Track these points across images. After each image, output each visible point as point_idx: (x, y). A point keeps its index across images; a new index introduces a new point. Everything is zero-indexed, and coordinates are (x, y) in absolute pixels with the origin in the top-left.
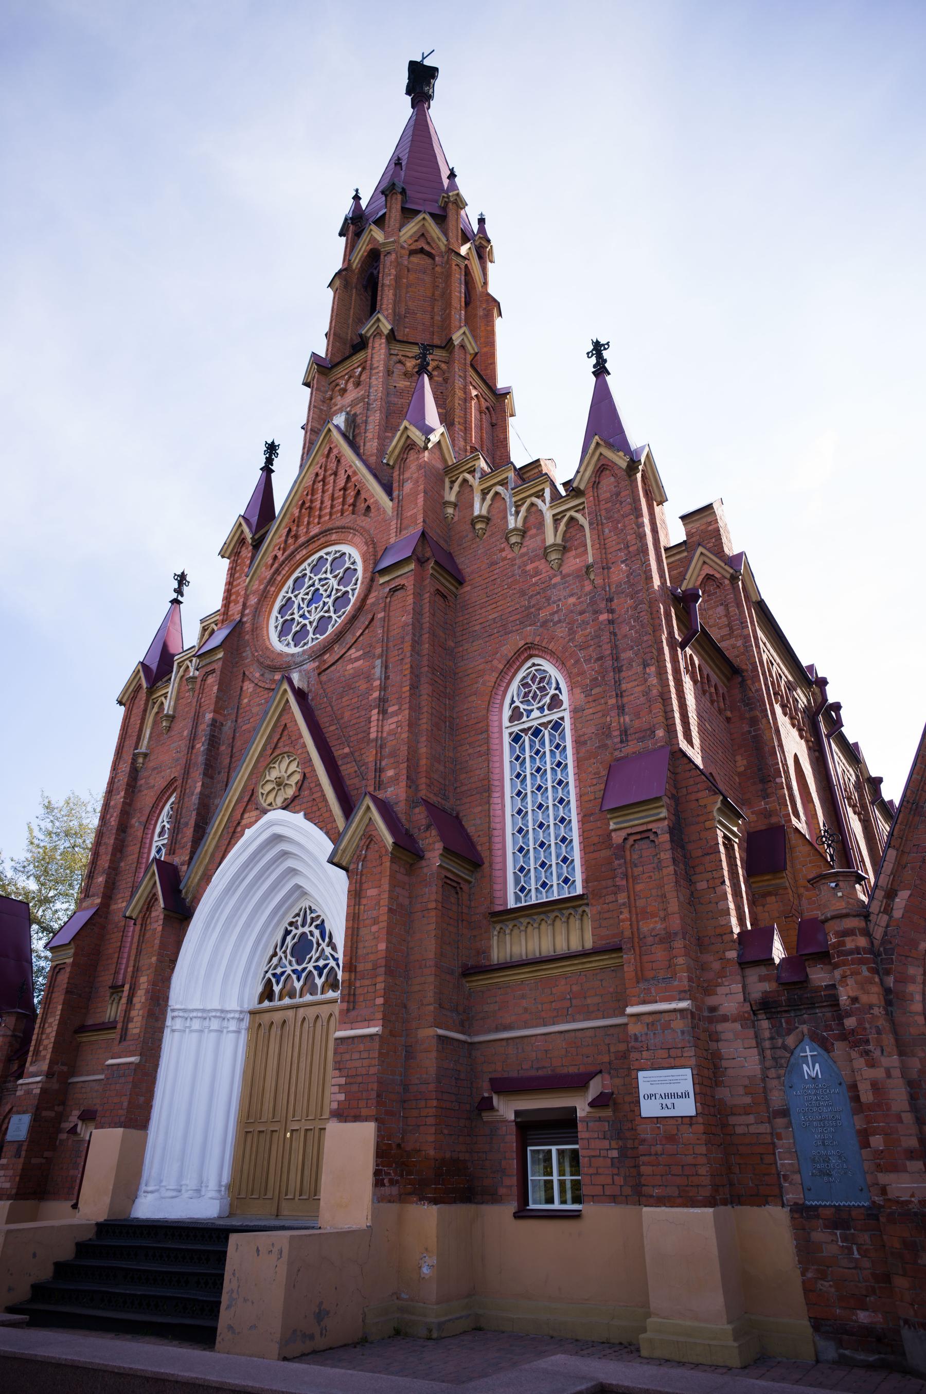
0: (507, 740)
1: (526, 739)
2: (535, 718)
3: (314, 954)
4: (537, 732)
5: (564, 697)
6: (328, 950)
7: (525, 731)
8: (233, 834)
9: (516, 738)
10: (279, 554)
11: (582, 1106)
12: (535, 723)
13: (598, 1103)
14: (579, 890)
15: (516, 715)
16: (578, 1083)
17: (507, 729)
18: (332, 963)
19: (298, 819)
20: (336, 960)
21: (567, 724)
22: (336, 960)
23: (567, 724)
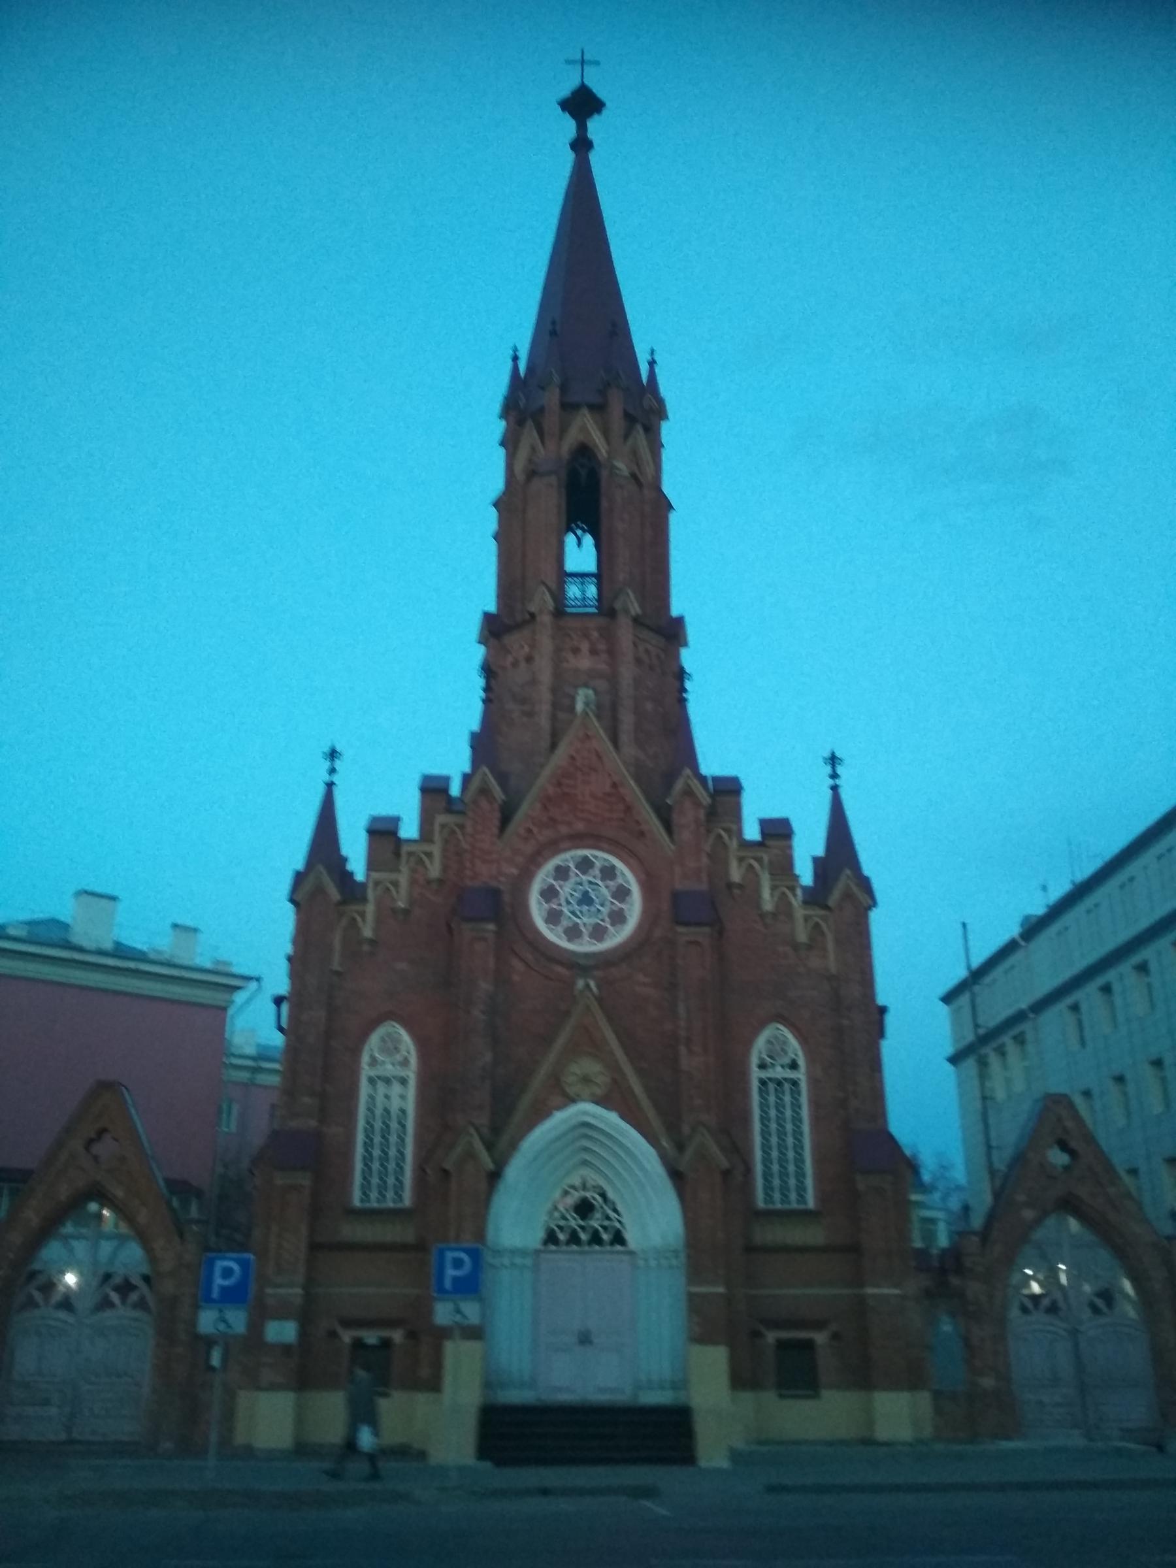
0: (755, 1085)
1: (771, 1086)
2: (779, 1072)
3: (598, 1215)
4: (779, 1083)
5: (801, 1062)
6: (612, 1215)
7: (770, 1079)
8: (540, 1113)
9: (763, 1082)
10: (535, 830)
11: (820, 1338)
12: (779, 1076)
13: (836, 1336)
14: (811, 1203)
15: (762, 1066)
16: (819, 1325)
17: (756, 1074)
18: (618, 1225)
19: (613, 1117)
20: (620, 1222)
21: (804, 1086)
22: (620, 1222)
23: (804, 1086)
